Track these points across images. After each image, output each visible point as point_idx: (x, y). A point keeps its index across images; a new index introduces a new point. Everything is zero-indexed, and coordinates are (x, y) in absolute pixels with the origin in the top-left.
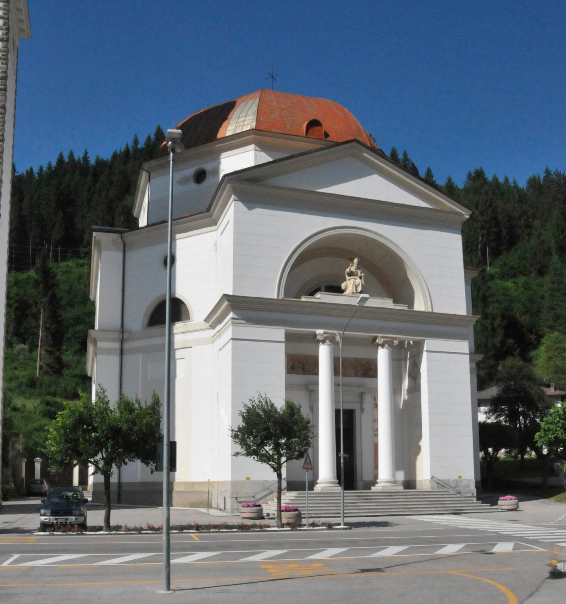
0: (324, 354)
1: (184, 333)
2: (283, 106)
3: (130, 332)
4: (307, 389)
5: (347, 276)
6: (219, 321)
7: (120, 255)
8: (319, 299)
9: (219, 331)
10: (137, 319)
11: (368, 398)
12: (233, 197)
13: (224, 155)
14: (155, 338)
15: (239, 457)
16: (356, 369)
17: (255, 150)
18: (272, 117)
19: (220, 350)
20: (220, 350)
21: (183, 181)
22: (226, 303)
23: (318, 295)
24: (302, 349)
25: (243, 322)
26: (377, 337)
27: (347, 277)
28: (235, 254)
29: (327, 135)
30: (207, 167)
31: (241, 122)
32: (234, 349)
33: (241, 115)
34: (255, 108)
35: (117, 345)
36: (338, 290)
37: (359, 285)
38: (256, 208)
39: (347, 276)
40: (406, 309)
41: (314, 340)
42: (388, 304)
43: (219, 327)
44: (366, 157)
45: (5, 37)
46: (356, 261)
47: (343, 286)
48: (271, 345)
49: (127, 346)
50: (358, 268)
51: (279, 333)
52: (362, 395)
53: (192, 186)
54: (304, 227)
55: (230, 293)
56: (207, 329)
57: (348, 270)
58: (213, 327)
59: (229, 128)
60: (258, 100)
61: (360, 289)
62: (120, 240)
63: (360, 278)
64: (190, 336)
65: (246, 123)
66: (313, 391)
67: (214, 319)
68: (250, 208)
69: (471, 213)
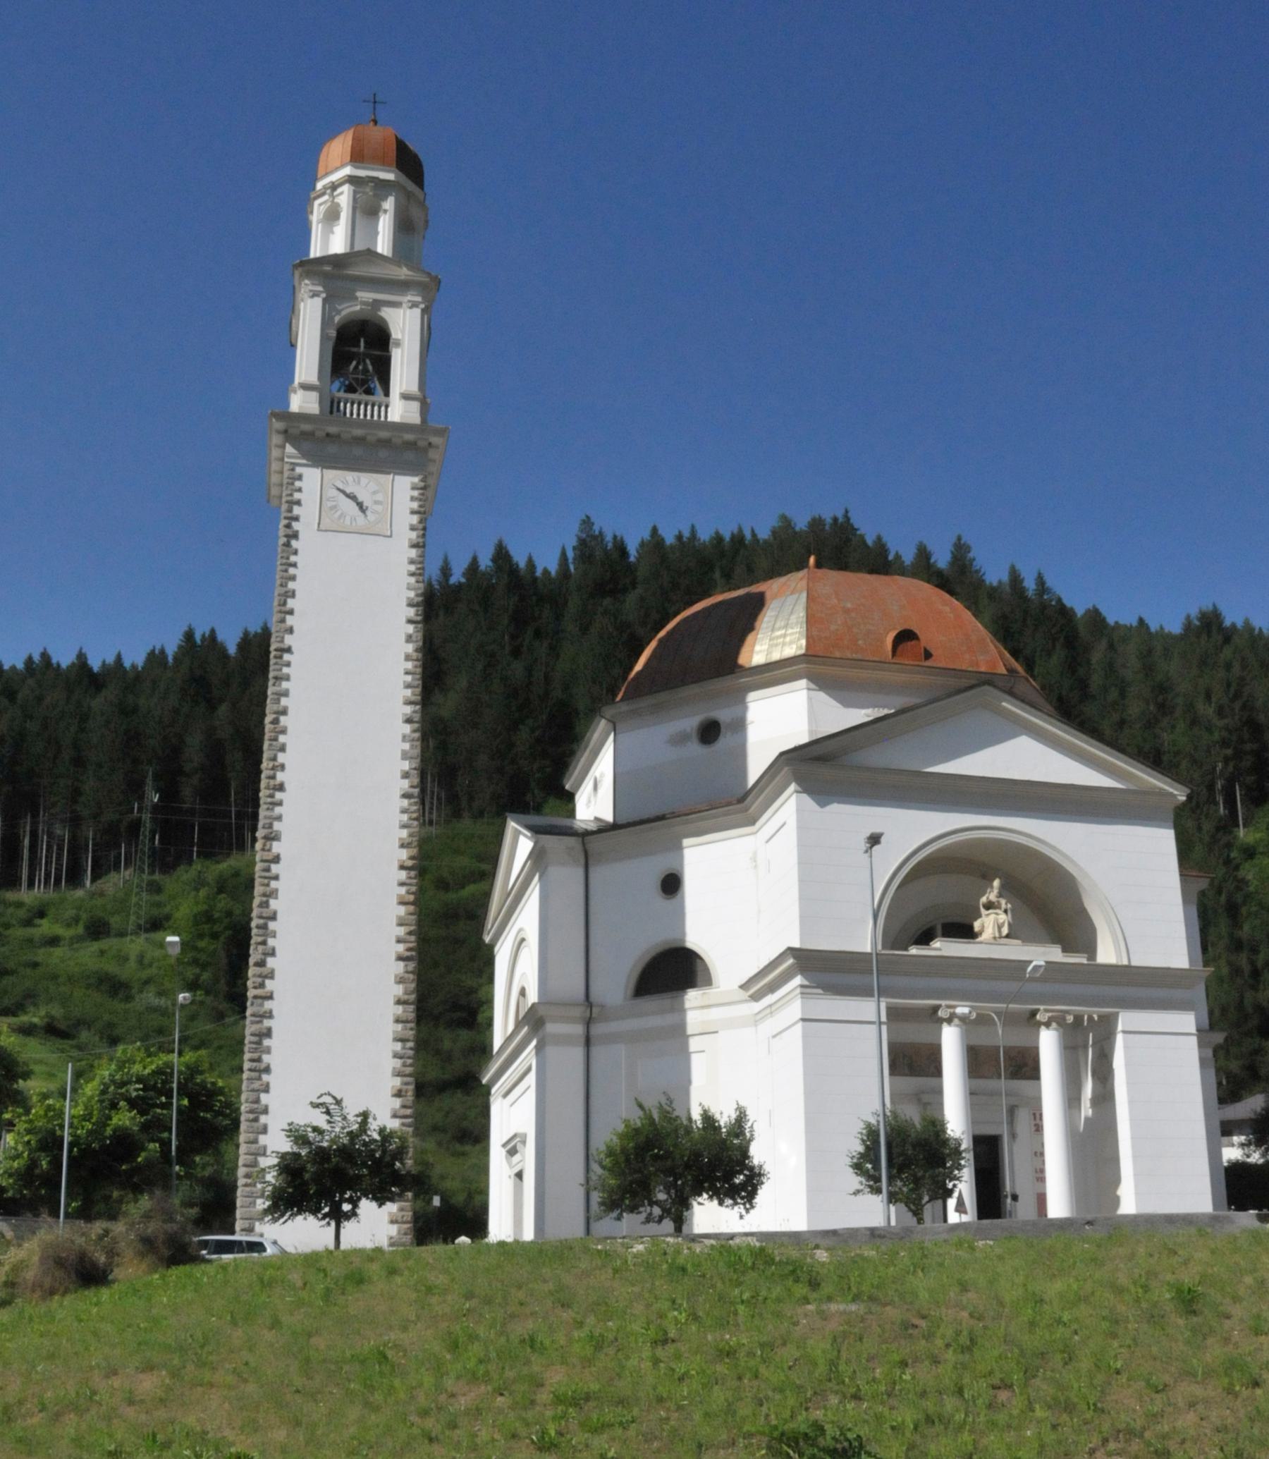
0: (951, 1042)
1: (703, 1007)
2: (849, 605)
3: (603, 1006)
4: (919, 1100)
5: (982, 910)
6: (772, 988)
7: (580, 872)
8: (939, 949)
9: (770, 1006)
10: (614, 982)
11: (1023, 1116)
12: (793, 787)
13: (752, 696)
14: (652, 1013)
15: (860, 1197)
16: (1003, 1065)
17: (809, 689)
18: (833, 627)
19: (774, 1036)
20: (774, 1036)
21: (679, 739)
22: (791, 961)
23: (937, 944)
24: (914, 1033)
25: (820, 991)
26: (1038, 1010)
27: (983, 911)
28: (802, 881)
29: (928, 655)
30: (723, 715)
31: (778, 637)
32: (805, 1036)
33: (777, 625)
34: (801, 613)
35: (579, 1029)
36: (964, 931)
37: (1003, 924)
38: (832, 802)
39: (982, 910)
40: (1085, 961)
41: (933, 1018)
42: (1055, 954)
43: (769, 999)
44: (1005, 708)
45: (421, 540)
46: (996, 883)
47: (977, 925)
48: (862, 1026)
49: (597, 1029)
50: (1000, 895)
51: (867, 1008)
52: (1012, 1111)
53: (695, 749)
54: (914, 830)
55: (797, 944)
56: (746, 1001)
57: (984, 900)
58: (756, 997)
59: (757, 648)
60: (804, 595)
61: (1005, 931)
62: (579, 847)
63: (1006, 911)
64: (715, 1014)
65: (788, 639)
66: (929, 1104)
67: (761, 985)
68: (822, 804)
69: (1188, 791)
